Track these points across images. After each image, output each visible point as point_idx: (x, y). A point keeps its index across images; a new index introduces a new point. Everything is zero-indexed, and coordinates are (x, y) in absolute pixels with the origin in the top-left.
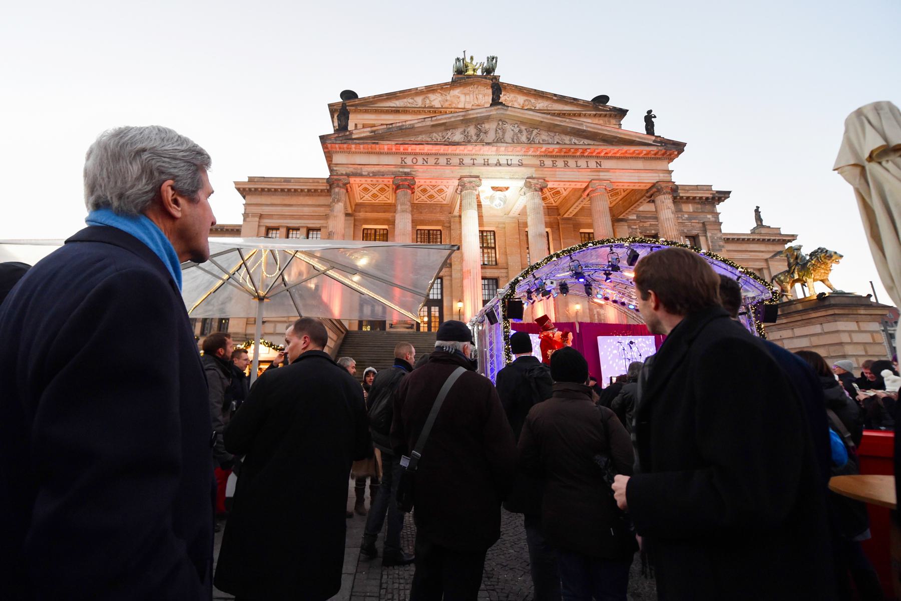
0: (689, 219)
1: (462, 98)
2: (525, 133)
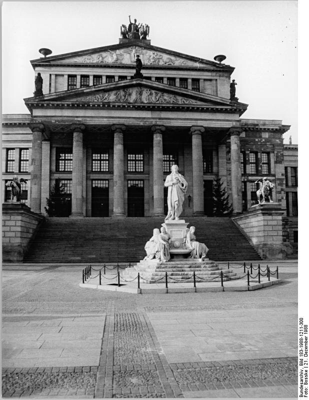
2: (154, 95)
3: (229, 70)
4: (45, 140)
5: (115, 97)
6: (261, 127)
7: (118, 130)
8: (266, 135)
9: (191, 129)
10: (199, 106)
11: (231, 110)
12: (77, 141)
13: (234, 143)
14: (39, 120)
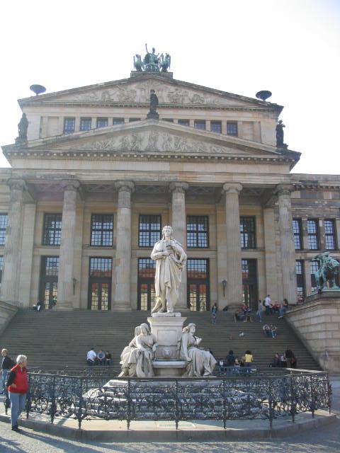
0: (328, 206)
1: (139, 92)
2: (173, 141)
3: (277, 109)
4: (30, 202)
5: (121, 143)
6: (321, 185)
7: (123, 188)
8: (329, 196)
9: (224, 186)
10: (234, 156)
11: (278, 160)
12: (69, 203)
13: (284, 205)
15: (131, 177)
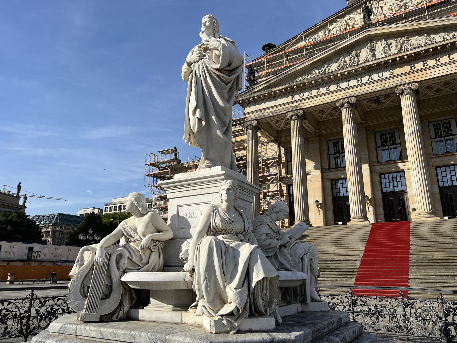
7: (345, 105)
14: (252, 116)
15: (353, 93)
